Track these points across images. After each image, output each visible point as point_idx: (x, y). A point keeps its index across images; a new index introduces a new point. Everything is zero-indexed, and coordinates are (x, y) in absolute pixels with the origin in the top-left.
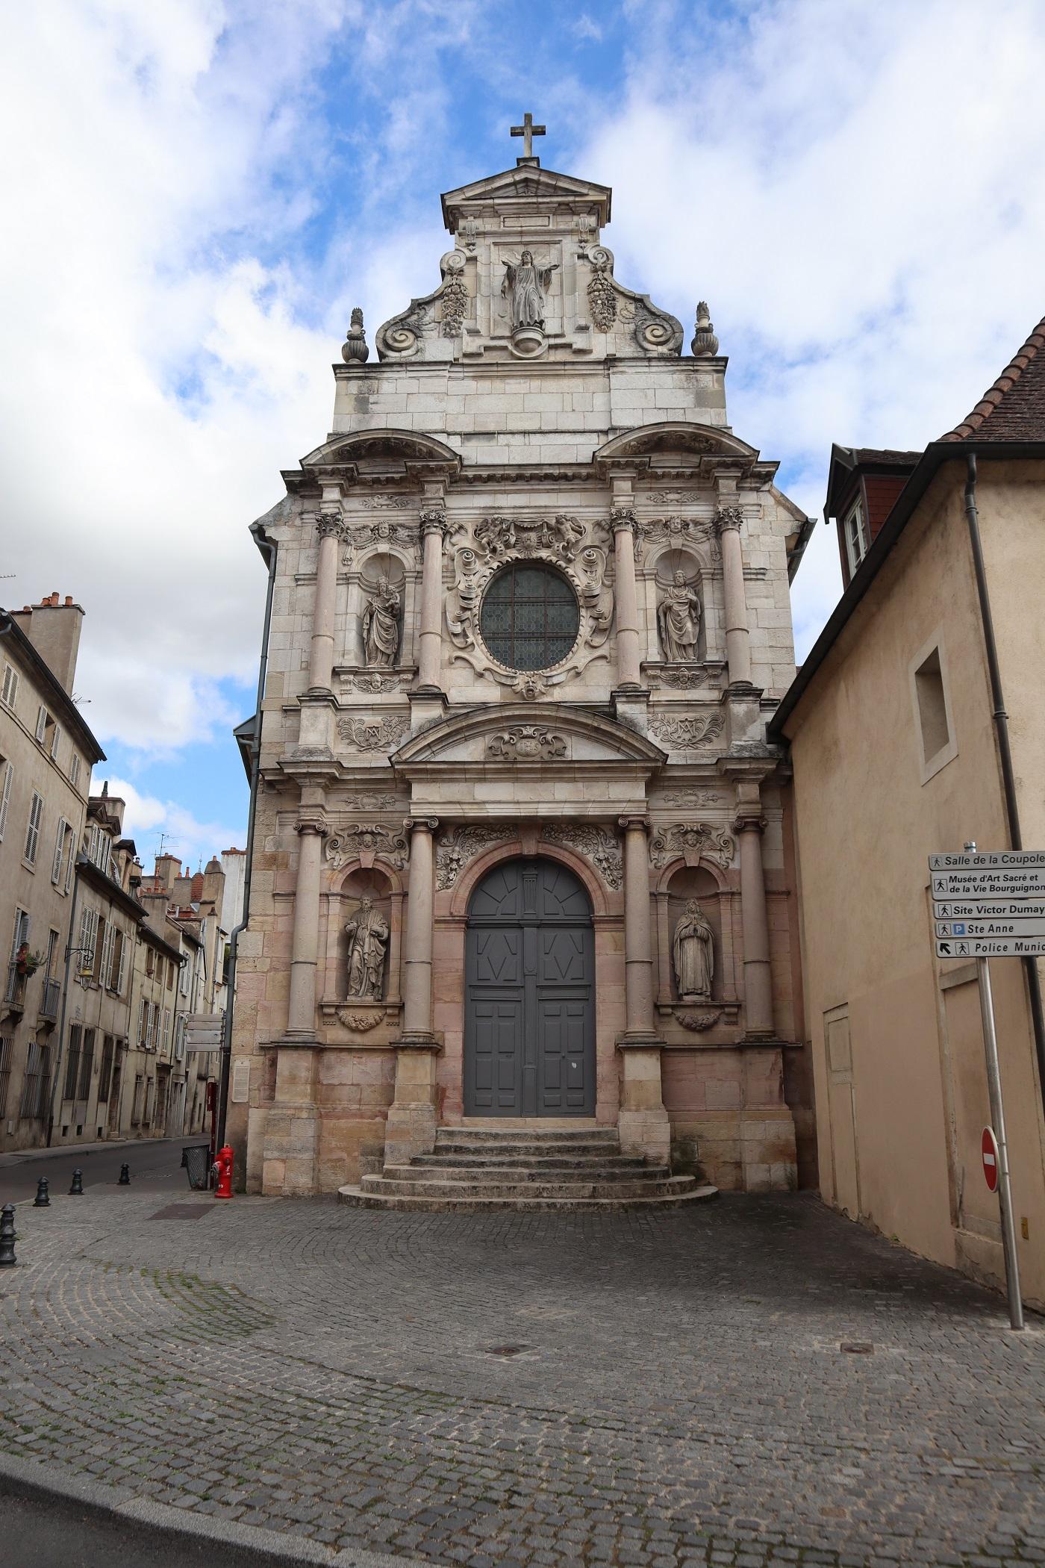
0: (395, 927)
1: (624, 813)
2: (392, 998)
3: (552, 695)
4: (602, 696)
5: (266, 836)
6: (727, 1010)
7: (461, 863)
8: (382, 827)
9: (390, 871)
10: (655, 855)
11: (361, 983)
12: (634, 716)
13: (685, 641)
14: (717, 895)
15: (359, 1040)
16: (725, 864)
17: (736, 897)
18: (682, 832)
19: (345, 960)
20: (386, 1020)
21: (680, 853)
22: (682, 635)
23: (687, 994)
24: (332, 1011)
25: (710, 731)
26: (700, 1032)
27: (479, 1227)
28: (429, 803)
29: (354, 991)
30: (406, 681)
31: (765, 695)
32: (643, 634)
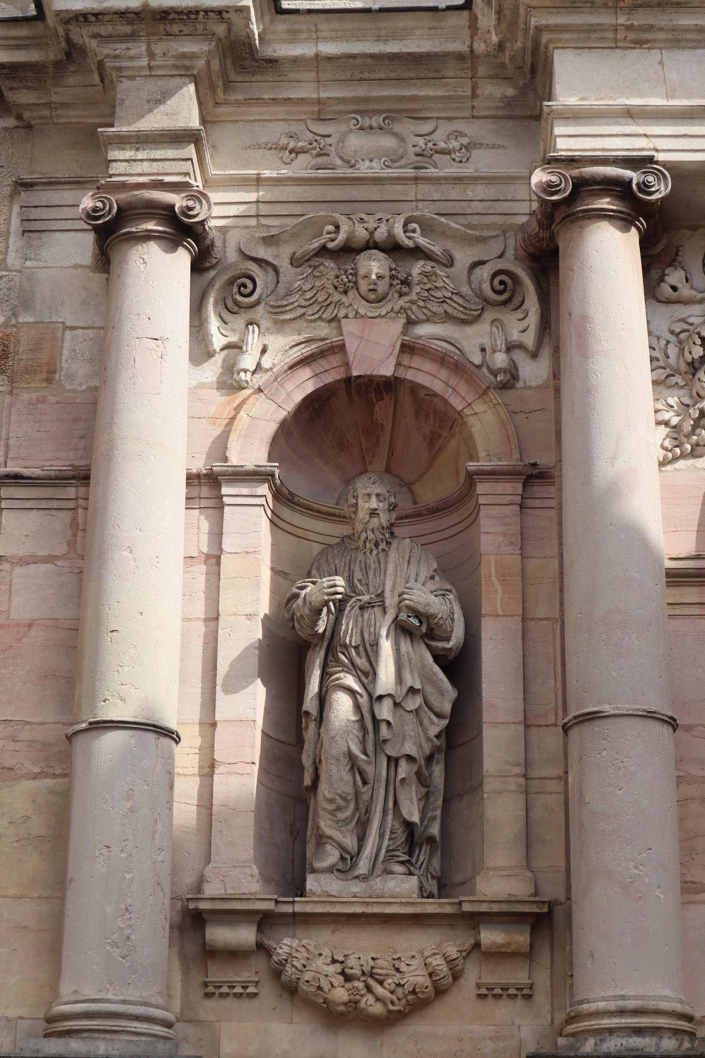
8: (427, 228)
9: (463, 389)
29: (332, 856)
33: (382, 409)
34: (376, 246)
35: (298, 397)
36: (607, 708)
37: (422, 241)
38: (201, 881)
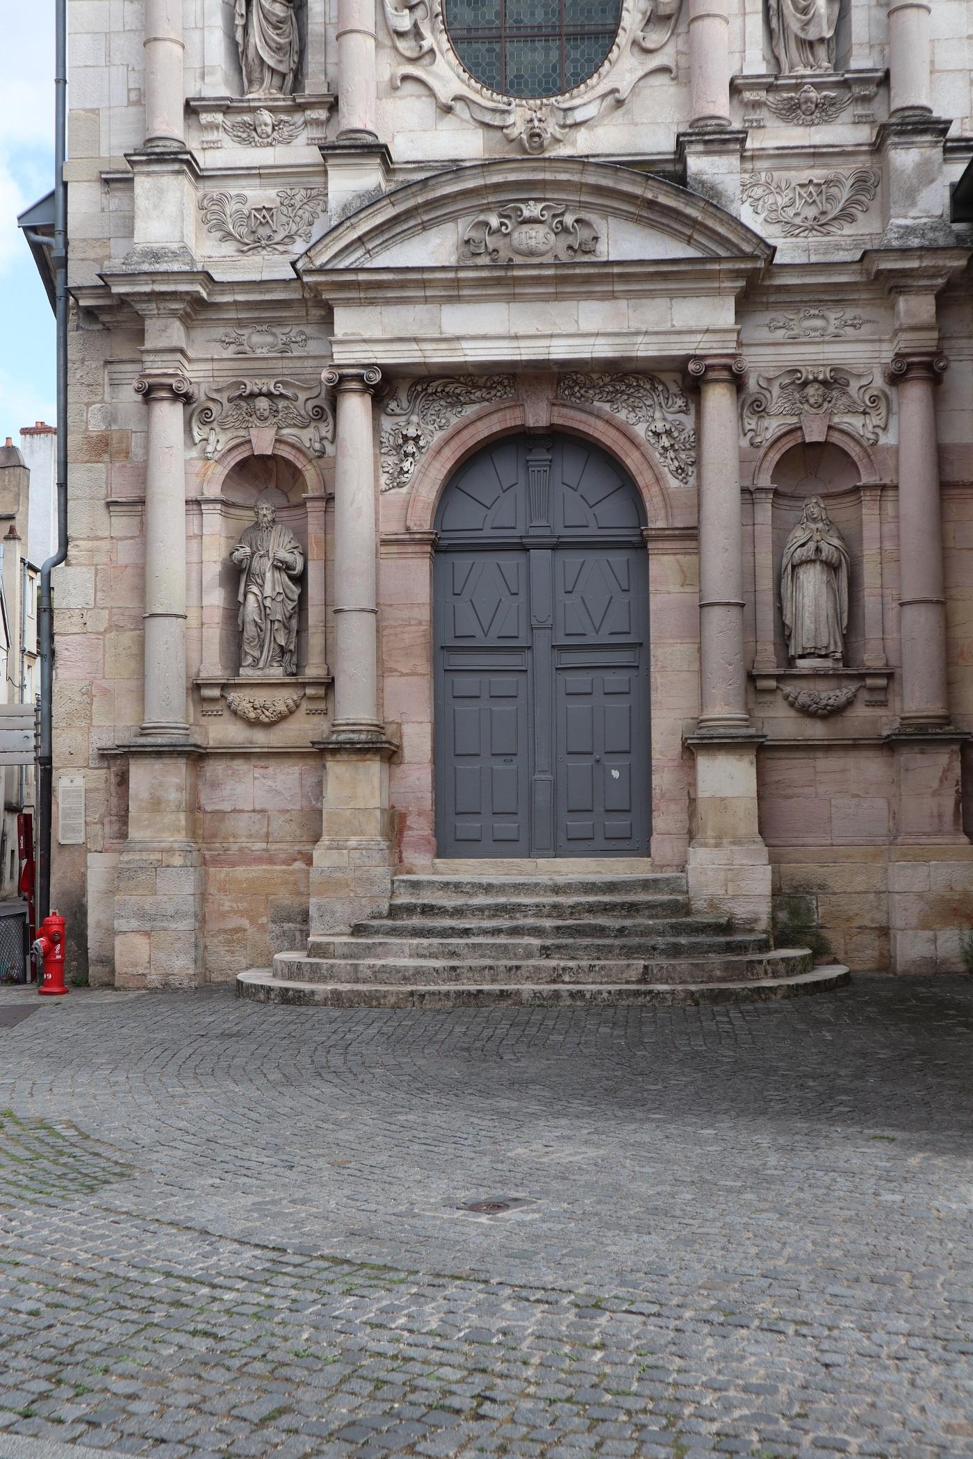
0: (314, 552)
1: (698, 352)
2: (313, 670)
3: (574, 144)
4: (660, 142)
5: (88, 405)
6: (869, 682)
7: (422, 443)
8: (285, 384)
9: (302, 458)
10: (751, 423)
11: (262, 647)
12: (718, 179)
13: (812, 34)
14: (856, 490)
15: (261, 738)
16: (872, 436)
17: (890, 493)
18: (798, 382)
19: (234, 610)
20: (305, 705)
21: (795, 420)
22: (807, 23)
23: (802, 657)
24: (216, 693)
25: (852, 202)
26: (823, 718)
27: (459, 1029)
28: (365, 341)
29: (249, 660)
30: (317, 123)
31: (953, 132)
32: (736, 23)
33: (270, 463)
34: (263, 395)
35: (233, 464)
36: (346, 608)
37: (283, 391)
38: (199, 671)
